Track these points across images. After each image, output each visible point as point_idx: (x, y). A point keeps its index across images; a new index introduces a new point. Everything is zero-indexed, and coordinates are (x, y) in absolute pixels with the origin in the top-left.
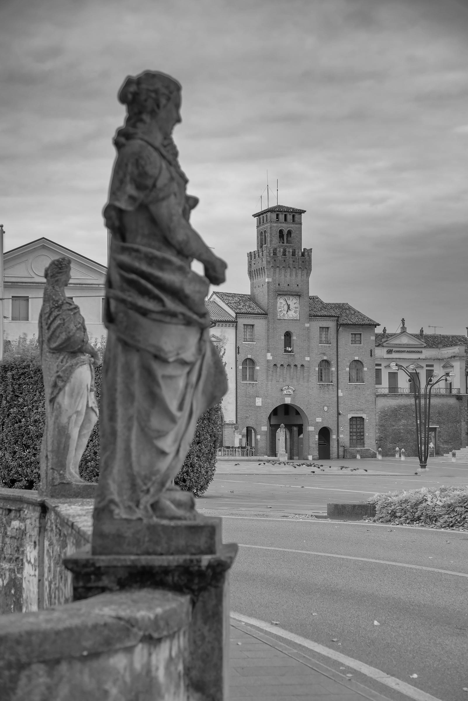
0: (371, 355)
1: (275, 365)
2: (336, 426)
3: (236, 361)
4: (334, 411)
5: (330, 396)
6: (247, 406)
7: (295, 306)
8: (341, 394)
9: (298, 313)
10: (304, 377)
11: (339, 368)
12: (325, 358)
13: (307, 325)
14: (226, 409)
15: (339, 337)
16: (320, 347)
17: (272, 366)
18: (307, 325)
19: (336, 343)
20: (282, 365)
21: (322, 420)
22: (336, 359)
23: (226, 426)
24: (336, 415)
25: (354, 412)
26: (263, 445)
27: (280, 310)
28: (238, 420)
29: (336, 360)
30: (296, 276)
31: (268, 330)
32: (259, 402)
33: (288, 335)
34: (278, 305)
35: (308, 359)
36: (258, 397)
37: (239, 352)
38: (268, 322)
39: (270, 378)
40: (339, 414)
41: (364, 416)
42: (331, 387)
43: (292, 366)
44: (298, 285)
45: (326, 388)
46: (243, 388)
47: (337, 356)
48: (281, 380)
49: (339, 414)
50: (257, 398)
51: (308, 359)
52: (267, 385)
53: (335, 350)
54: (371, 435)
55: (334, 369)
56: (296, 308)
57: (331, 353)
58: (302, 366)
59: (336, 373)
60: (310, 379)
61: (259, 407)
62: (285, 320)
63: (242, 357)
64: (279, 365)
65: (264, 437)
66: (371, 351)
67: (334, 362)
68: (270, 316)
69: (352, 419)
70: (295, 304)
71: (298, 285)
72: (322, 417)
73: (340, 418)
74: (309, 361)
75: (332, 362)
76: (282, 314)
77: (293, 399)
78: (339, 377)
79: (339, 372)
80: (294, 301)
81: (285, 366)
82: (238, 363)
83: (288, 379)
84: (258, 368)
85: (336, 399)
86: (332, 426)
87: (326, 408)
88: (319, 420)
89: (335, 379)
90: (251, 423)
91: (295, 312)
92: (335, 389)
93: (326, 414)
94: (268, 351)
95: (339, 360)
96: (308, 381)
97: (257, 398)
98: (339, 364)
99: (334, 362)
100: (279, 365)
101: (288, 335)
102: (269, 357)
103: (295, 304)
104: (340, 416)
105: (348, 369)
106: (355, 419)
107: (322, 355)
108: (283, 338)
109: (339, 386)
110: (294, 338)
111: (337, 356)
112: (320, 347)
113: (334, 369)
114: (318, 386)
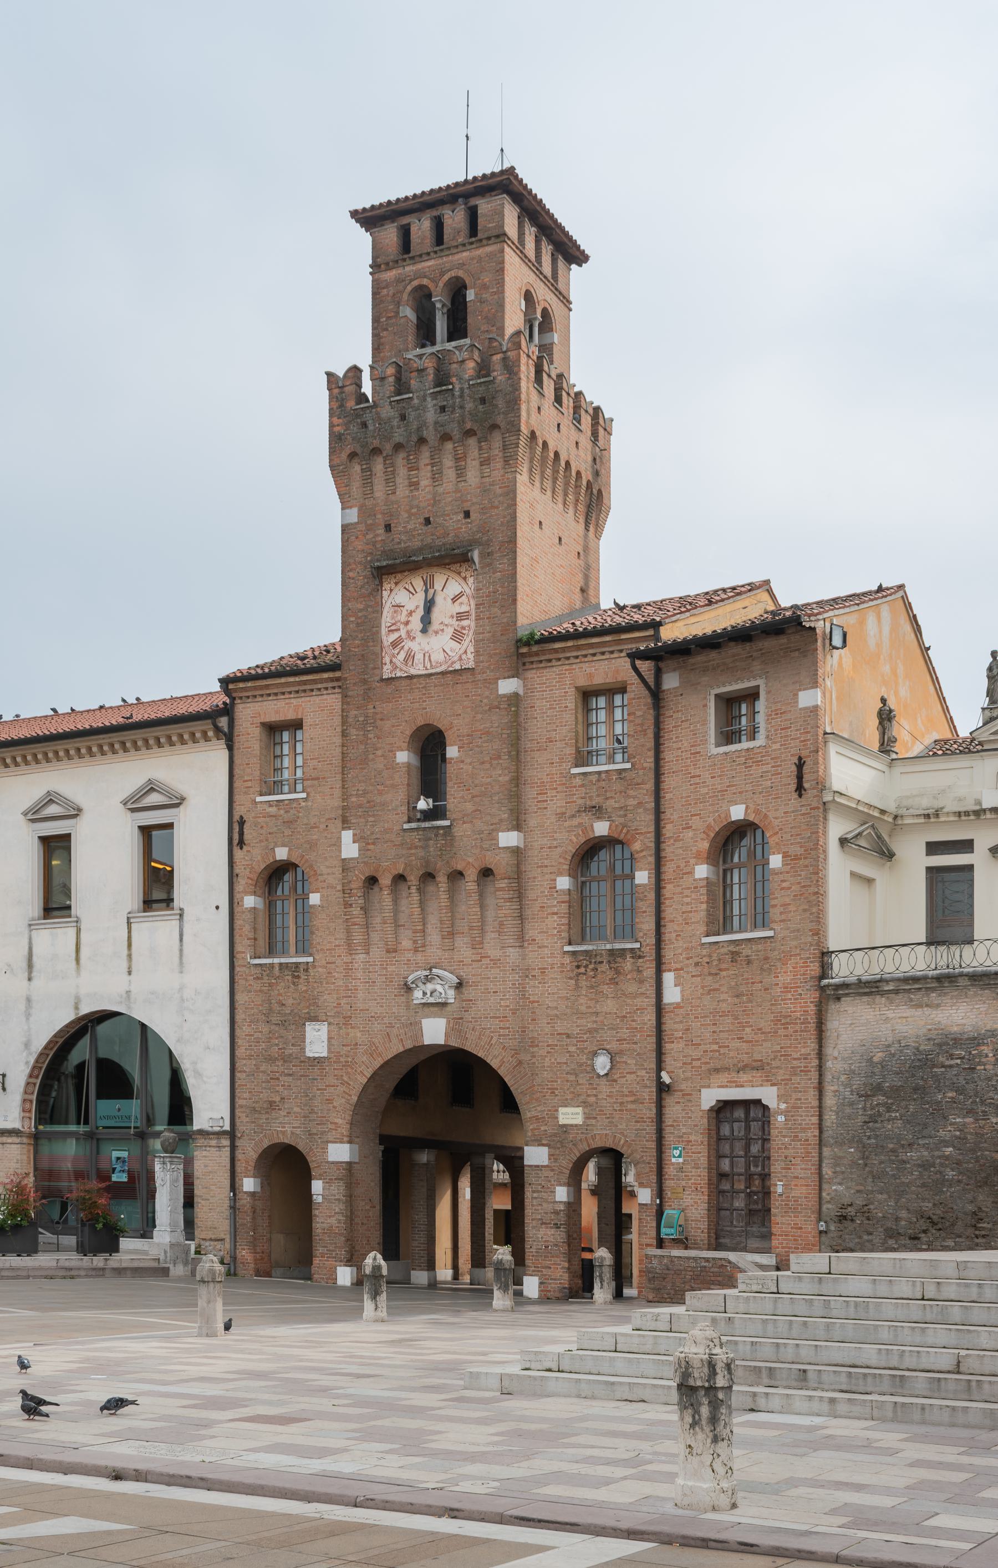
0: (800, 789)
1: (372, 881)
2: (653, 1145)
3: (232, 877)
4: (638, 1078)
5: (624, 1006)
6: (271, 1060)
7: (457, 608)
8: (672, 994)
9: (468, 644)
10: (501, 924)
11: (669, 870)
12: (601, 828)
13: (507, 686)
14: (198, 1074)
15: (669, 724)
16: (578, 781)
17: (357, 883)
18: (507, 686)
19: (651, 753)
20: (400, 878)
21: (587, 1117)
22: (652, 828)
23: (201, 1141)
24: (649, 1094)
25: (723, 1078)
26: (333, 1221)
27: (393, 637)
28: (242, 1117)
29: (652, 836)
30: (436, 477)
31: (344, 734)
32: (317, 1041)
33: (430, 745)
34: (387, 617)
35: (509, 839)
36: (315, 1019)
37: (241, 843)
38: (345, 696)
39: (358, 937)
40: (663, 1089)
41: (769, 1095)
42: (628, 964)
43: (442, 878)
44: (467, 514)
45: (605, 967)
46: (257, 985)
47: (658, 812)
48: (406, 943)
49: (663, 1089)
50: (310, 1028)
51: (509, 839)
52: (348, 968)
53: (650, 785)
54: (796, 1193)
55: (642, 877)
56: (460, 616)
57: (632, 802)
58: (486, 873)
59: (652, 896)
60: (531, 933)
61: (318, 1061)
62: (411, 677)
63: (254, 860)
64: (386, 881)
65: (338, 1190)
66: (800, 765)
67: (642, 844)
68: (350, 673)
69: (724, 1108)
70: (454, 600)
71: (467, 514)
72: (585, 1104)
73: (673, 1109)
74: (516, 852)
75: (637, 846)
76: (402, 656)
77: (455, 1026)
78: (669, 912)
79: (668, 890)
80: (455, 587)
81: (413, 879)
82: (241, 885)
83: (434, 937)
84: (315, 899)
85: (650, 1017)
86: (638, 1146)
87: (602, 1063)
88: (571, 1116)
89: (647, 924)
90: (286, 1129)
91: (457, 636)
92: (650, 972)
93: (604, 1088)
94: (346, 823)
95: (668, 830)
96: (521, 939)
97: (310, 1028)
98: (668, 850)
99: (642, 844)
100: (386, 881)
101: (430, 745)
102: (350, 848)
103: (454, 600)
104: (669, 1101)
105: (702, 871)
106: (739, 1113)
107: (585, 818)
108: (403, 757)
109: (668, 954)
110: (452, 752)
111: (658, 813)
112: (578, 781)
113: (642, 877)
114: (567, 960)
